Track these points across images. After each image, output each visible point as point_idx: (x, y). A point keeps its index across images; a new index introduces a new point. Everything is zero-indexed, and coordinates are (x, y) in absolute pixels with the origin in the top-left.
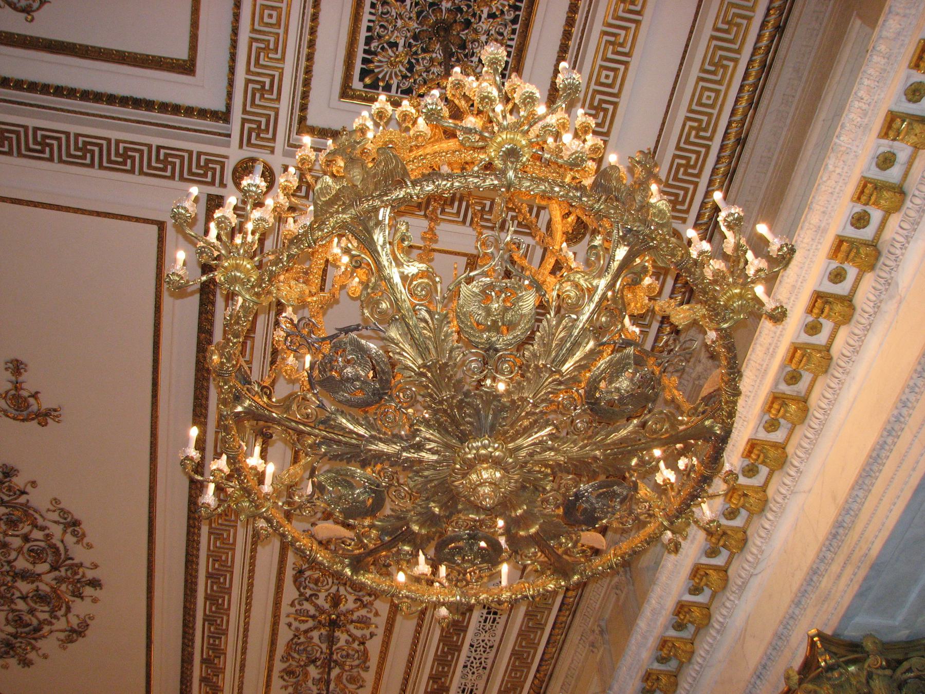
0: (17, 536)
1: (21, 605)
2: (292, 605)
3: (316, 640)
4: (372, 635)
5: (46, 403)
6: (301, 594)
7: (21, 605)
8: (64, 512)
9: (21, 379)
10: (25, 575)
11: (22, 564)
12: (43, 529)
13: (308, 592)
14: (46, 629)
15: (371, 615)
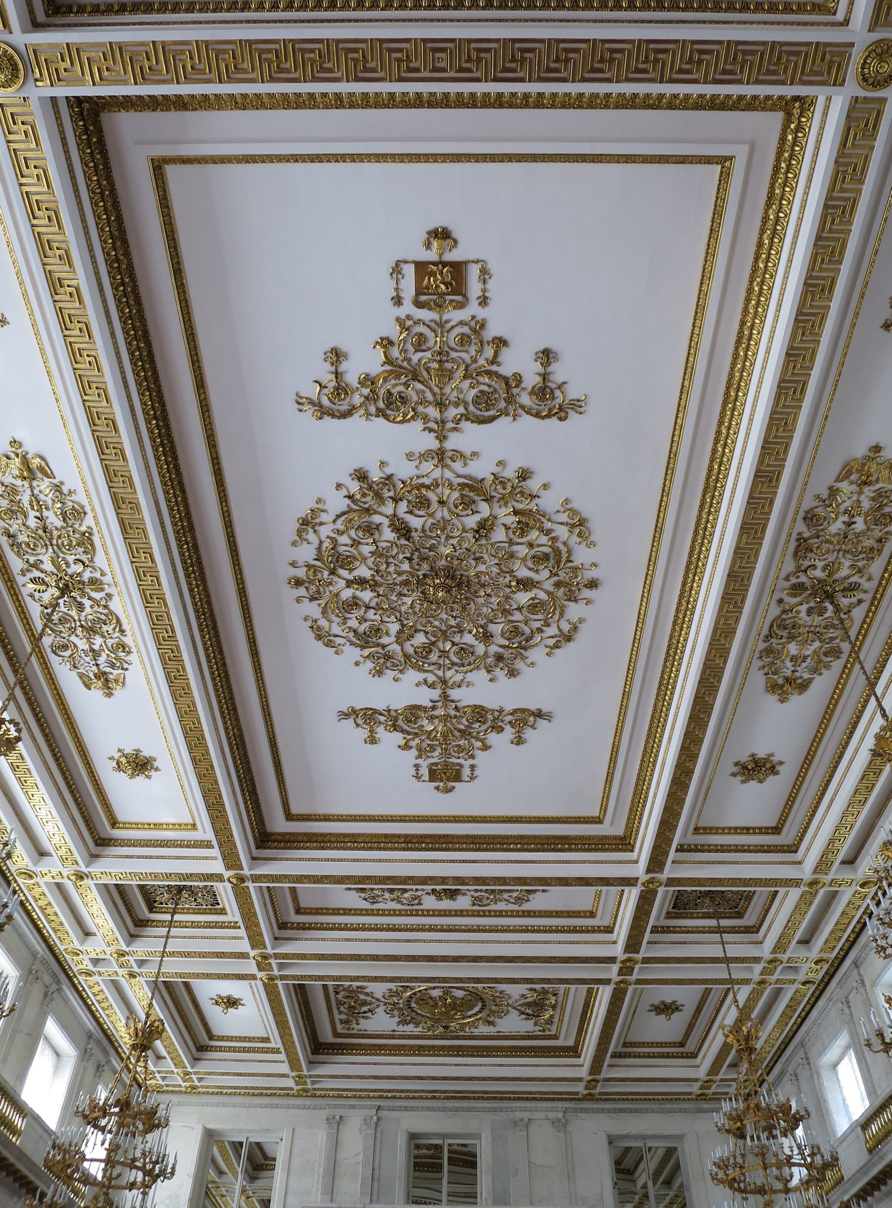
0: (521, 544)
1: (517, 616)
2: (787, 579)
3: (803, 615)
4: (860, 601)
5: (573, 392)
6: (798, 567)
7: (517, 616)
8: (573, 512)
9: (549, 369)
10: (526, 584)
11: (523, 573)
12: (548, 532)
13: (806, 563)
14: (537, 638)
15: (862, 581)
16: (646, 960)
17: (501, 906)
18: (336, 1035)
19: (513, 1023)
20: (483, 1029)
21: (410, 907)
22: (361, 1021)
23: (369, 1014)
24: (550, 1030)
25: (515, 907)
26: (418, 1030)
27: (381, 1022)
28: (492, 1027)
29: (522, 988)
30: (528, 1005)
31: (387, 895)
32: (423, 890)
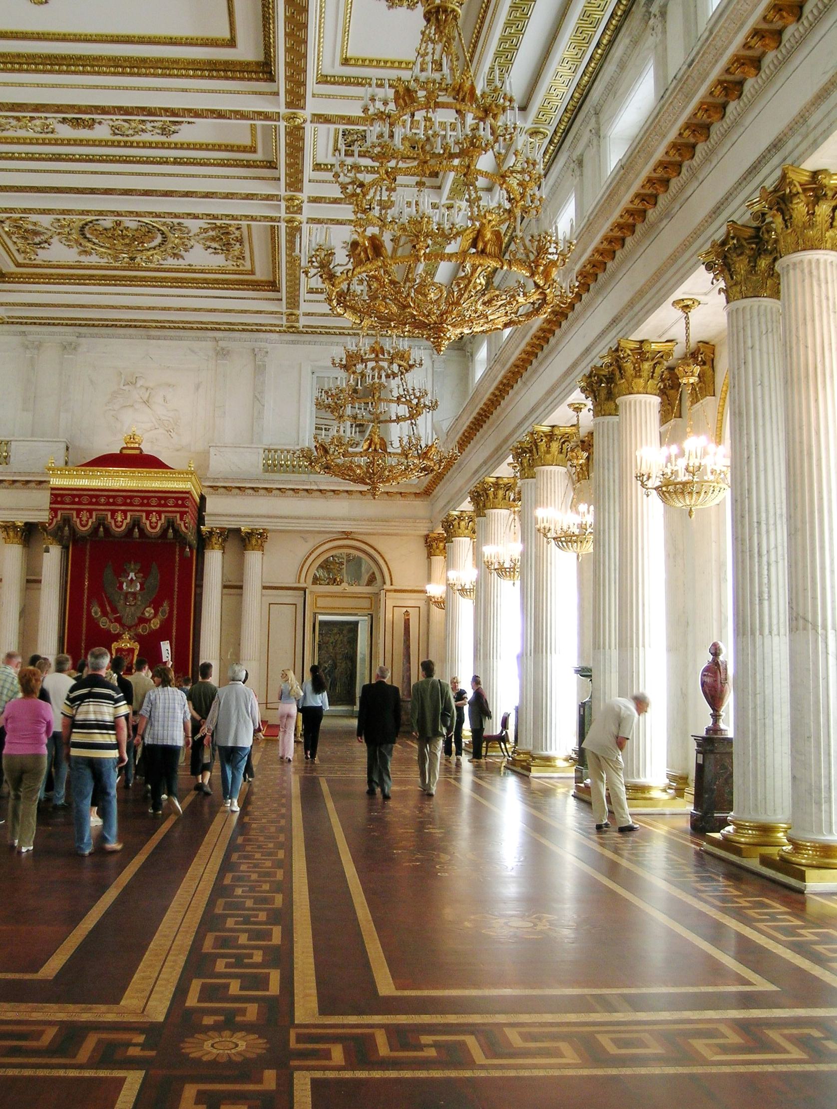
16: (315, 200)
17: (146, 137)
18: (18, 265)
19: (200, 257)
20: (171, 262)
21: (43, 136)
22: (39, 251)
23: (46, 245)
24: (243, 265)
25: (163, 139)
26: (103, 262)
27: (60, 252)
28: (180, 260)
29: (202, 223)
30: (213, 239)
31: (14, 123)
32: (55, 118)
